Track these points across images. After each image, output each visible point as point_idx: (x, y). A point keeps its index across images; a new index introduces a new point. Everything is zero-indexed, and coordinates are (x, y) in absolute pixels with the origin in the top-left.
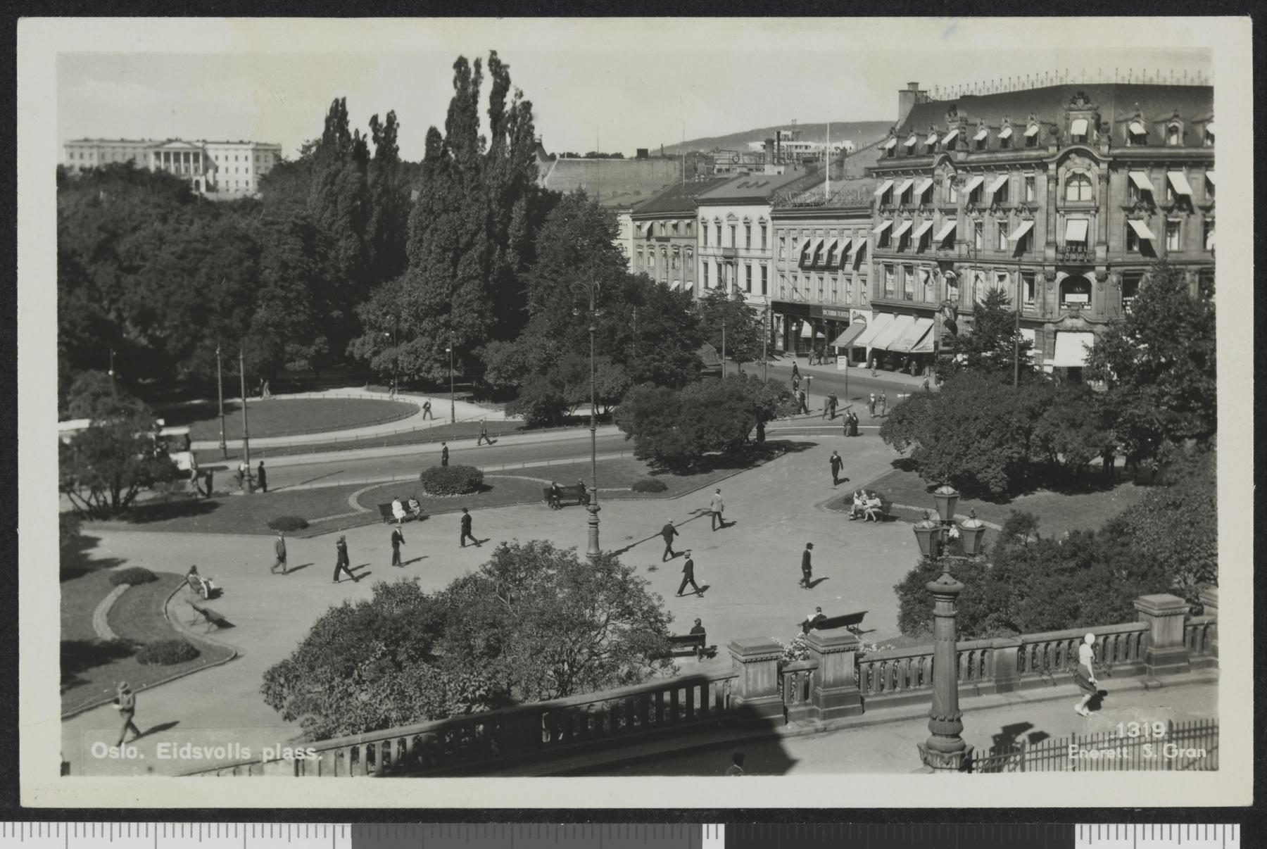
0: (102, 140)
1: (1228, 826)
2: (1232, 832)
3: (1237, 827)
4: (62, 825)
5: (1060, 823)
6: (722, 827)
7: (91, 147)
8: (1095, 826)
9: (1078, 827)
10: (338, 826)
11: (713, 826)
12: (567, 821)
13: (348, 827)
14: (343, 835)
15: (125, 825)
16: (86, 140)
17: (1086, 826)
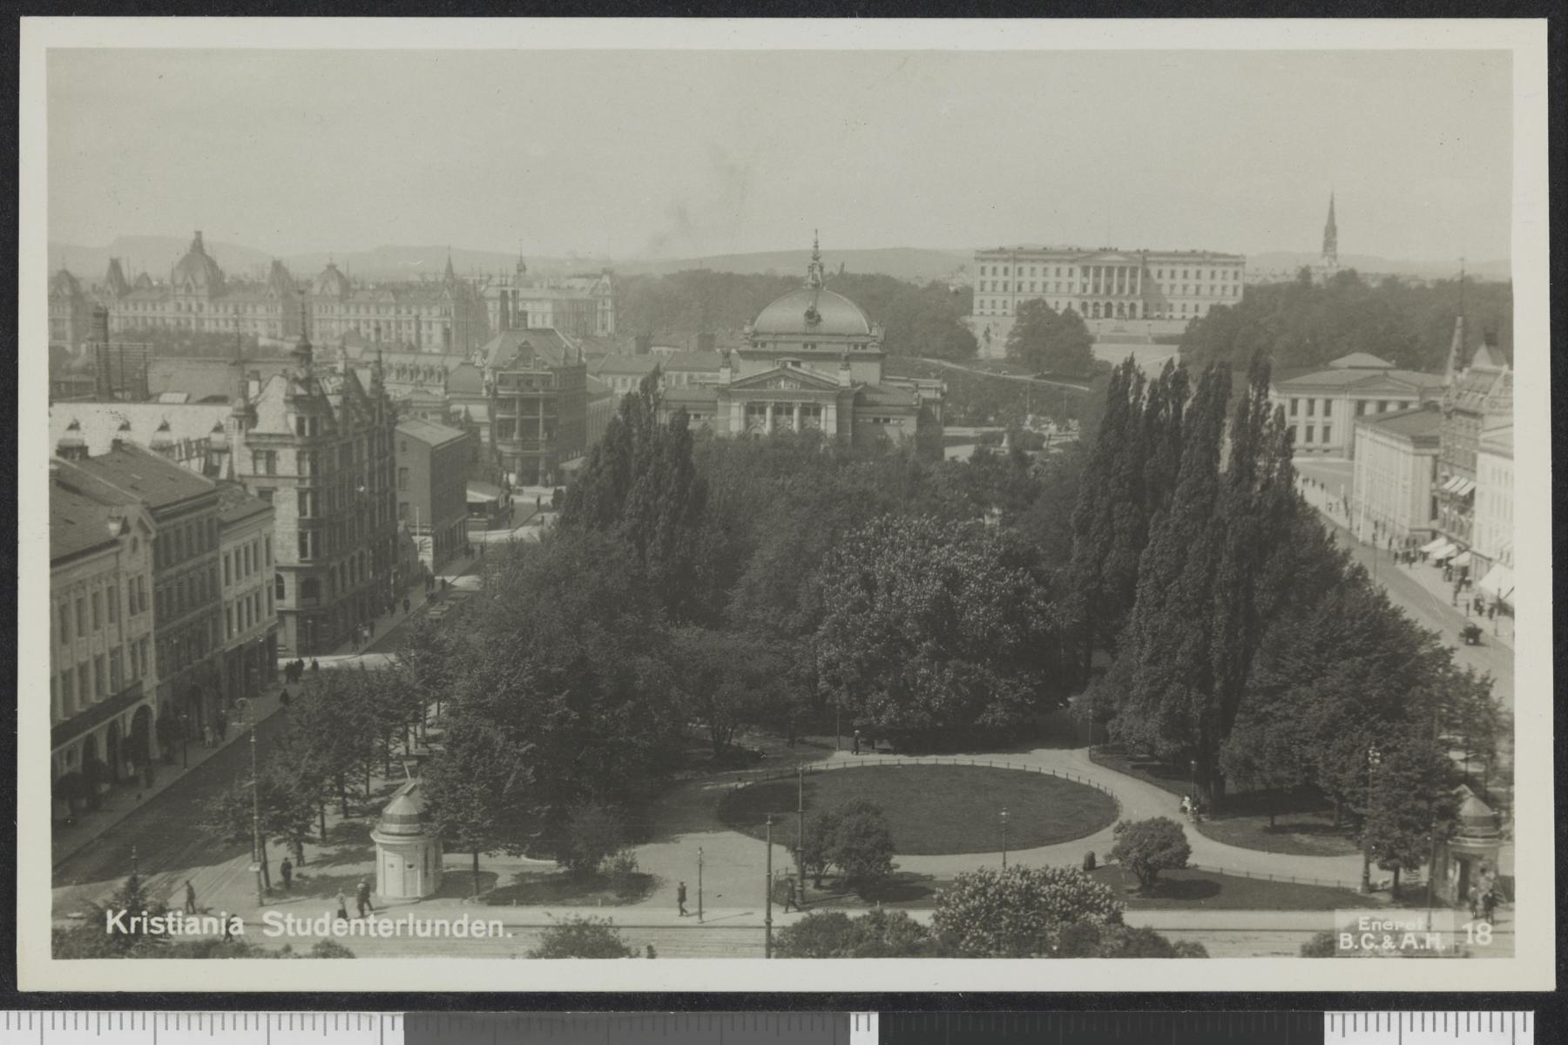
0: (1021, 250)
1: (1519, 1015)
2: (1525, 1022)
3: (1530, 1015)
4: (36, 1014)
5: (1305, 1012)
6: (875, 1017)
7: (1006, 260)
8: (1349, 1015)
9: (1327, 1016)
10: (387, 1016)
11: (863, 1017)
12: (678, 1008)
13: (399, 1018)
14: (393, 1026)
15: (127, 1014)
16: (1001, 250)
17: (1338, 1015)
